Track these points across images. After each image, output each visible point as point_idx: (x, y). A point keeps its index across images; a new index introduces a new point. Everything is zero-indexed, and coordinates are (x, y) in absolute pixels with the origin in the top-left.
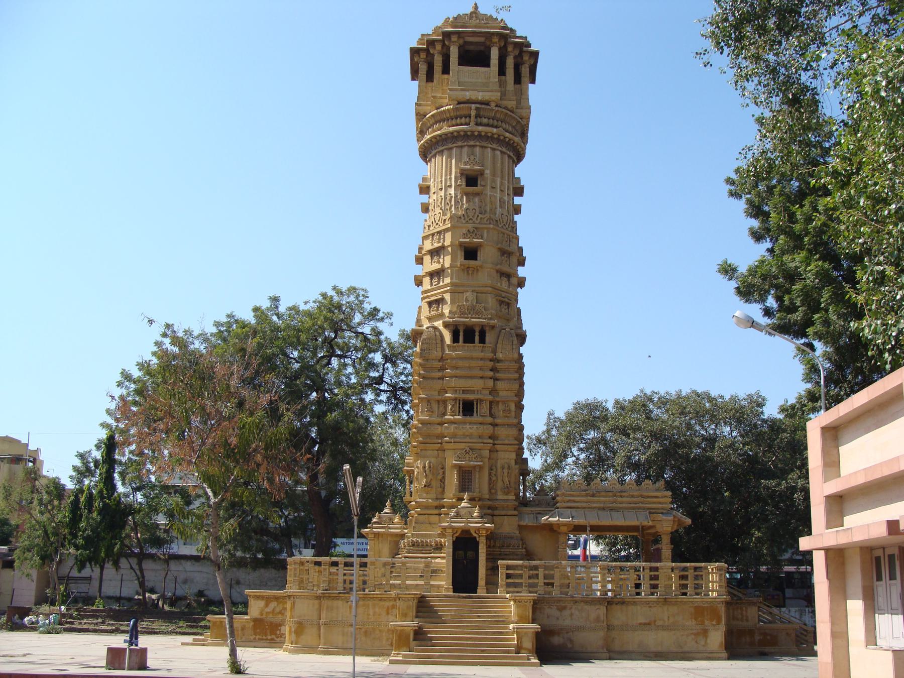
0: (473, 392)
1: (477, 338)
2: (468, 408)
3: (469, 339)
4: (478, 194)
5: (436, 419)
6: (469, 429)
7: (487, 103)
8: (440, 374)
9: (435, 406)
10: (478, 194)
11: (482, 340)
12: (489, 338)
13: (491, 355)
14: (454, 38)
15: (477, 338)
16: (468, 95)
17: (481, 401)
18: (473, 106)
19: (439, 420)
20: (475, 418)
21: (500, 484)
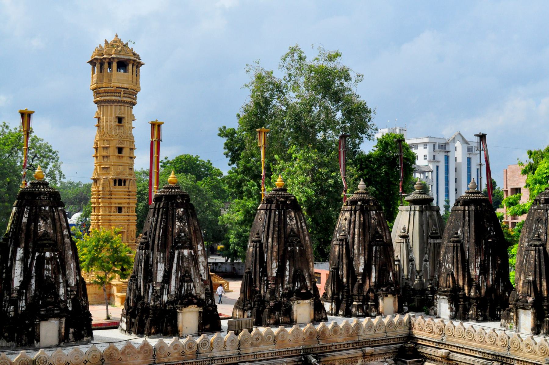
0: (122, 204)
1: (123, 184)
2: (120, 210)
3: (120, 184)
4: (122, 126)
5: (107, 213)
6: (120, 218)
7: (127, 89)
8: (109, 197)
9: (107, 209)
10: (122, 126)
11: (125, 185)
12: (127, 183)
13: (128, 190)
14: (116, 60)
15: (123, 184)
16: (121, 85)
17: (124, 207)
18: (123, 90)
19: (109, 214)
20: (123, 214)
21: (130, 237)
